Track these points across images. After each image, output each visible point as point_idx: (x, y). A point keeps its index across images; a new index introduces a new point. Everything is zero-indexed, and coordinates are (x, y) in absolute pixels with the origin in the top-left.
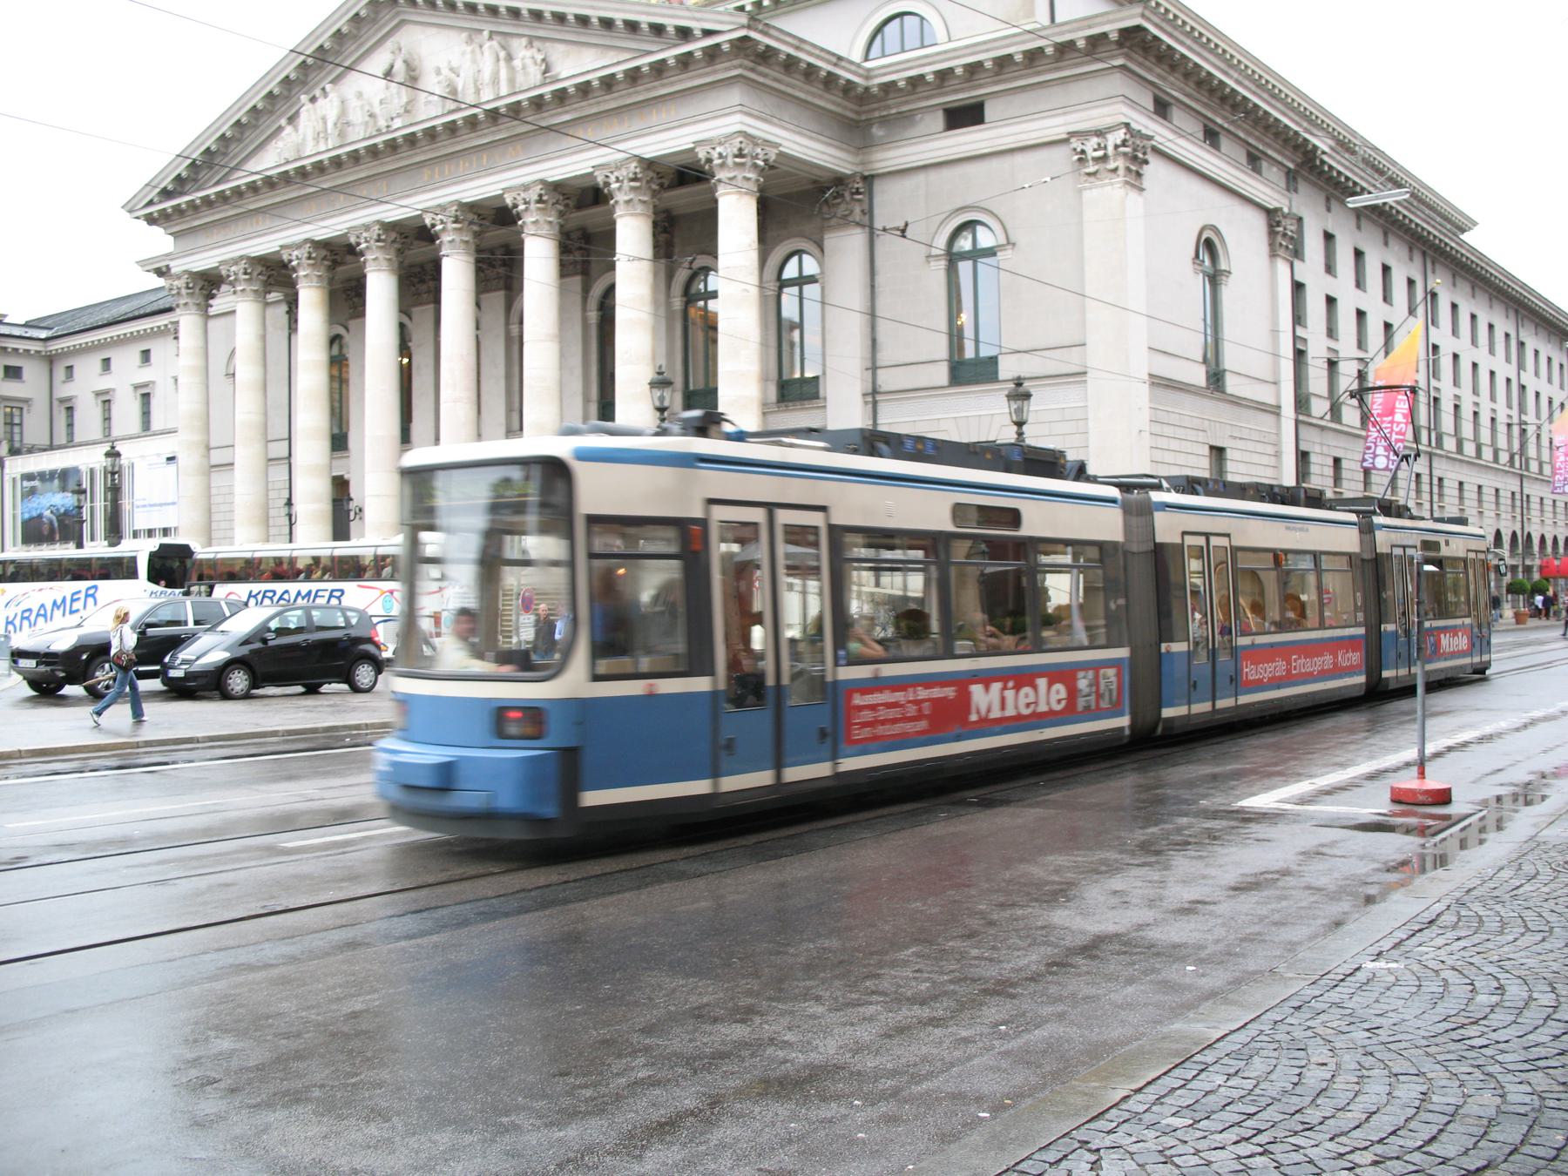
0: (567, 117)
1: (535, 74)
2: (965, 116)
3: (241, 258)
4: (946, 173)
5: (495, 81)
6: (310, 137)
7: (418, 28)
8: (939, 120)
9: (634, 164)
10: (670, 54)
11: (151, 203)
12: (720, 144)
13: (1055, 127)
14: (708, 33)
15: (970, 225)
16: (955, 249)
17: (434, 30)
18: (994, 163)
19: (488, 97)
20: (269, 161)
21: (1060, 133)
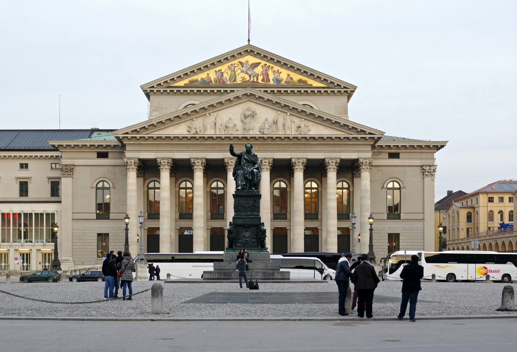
0: (316, 143)
2: (394, 156)
4: (387, 168)
6: (209, 127)
7: (254, 104)
8: (387, 156)
10: (359, 136)
11: (127, 133)
13: (419, 162)
15: (393, 181)
17: (261, 106)
18: (401, 168)
20: (180, 130)
21: (420, 164)
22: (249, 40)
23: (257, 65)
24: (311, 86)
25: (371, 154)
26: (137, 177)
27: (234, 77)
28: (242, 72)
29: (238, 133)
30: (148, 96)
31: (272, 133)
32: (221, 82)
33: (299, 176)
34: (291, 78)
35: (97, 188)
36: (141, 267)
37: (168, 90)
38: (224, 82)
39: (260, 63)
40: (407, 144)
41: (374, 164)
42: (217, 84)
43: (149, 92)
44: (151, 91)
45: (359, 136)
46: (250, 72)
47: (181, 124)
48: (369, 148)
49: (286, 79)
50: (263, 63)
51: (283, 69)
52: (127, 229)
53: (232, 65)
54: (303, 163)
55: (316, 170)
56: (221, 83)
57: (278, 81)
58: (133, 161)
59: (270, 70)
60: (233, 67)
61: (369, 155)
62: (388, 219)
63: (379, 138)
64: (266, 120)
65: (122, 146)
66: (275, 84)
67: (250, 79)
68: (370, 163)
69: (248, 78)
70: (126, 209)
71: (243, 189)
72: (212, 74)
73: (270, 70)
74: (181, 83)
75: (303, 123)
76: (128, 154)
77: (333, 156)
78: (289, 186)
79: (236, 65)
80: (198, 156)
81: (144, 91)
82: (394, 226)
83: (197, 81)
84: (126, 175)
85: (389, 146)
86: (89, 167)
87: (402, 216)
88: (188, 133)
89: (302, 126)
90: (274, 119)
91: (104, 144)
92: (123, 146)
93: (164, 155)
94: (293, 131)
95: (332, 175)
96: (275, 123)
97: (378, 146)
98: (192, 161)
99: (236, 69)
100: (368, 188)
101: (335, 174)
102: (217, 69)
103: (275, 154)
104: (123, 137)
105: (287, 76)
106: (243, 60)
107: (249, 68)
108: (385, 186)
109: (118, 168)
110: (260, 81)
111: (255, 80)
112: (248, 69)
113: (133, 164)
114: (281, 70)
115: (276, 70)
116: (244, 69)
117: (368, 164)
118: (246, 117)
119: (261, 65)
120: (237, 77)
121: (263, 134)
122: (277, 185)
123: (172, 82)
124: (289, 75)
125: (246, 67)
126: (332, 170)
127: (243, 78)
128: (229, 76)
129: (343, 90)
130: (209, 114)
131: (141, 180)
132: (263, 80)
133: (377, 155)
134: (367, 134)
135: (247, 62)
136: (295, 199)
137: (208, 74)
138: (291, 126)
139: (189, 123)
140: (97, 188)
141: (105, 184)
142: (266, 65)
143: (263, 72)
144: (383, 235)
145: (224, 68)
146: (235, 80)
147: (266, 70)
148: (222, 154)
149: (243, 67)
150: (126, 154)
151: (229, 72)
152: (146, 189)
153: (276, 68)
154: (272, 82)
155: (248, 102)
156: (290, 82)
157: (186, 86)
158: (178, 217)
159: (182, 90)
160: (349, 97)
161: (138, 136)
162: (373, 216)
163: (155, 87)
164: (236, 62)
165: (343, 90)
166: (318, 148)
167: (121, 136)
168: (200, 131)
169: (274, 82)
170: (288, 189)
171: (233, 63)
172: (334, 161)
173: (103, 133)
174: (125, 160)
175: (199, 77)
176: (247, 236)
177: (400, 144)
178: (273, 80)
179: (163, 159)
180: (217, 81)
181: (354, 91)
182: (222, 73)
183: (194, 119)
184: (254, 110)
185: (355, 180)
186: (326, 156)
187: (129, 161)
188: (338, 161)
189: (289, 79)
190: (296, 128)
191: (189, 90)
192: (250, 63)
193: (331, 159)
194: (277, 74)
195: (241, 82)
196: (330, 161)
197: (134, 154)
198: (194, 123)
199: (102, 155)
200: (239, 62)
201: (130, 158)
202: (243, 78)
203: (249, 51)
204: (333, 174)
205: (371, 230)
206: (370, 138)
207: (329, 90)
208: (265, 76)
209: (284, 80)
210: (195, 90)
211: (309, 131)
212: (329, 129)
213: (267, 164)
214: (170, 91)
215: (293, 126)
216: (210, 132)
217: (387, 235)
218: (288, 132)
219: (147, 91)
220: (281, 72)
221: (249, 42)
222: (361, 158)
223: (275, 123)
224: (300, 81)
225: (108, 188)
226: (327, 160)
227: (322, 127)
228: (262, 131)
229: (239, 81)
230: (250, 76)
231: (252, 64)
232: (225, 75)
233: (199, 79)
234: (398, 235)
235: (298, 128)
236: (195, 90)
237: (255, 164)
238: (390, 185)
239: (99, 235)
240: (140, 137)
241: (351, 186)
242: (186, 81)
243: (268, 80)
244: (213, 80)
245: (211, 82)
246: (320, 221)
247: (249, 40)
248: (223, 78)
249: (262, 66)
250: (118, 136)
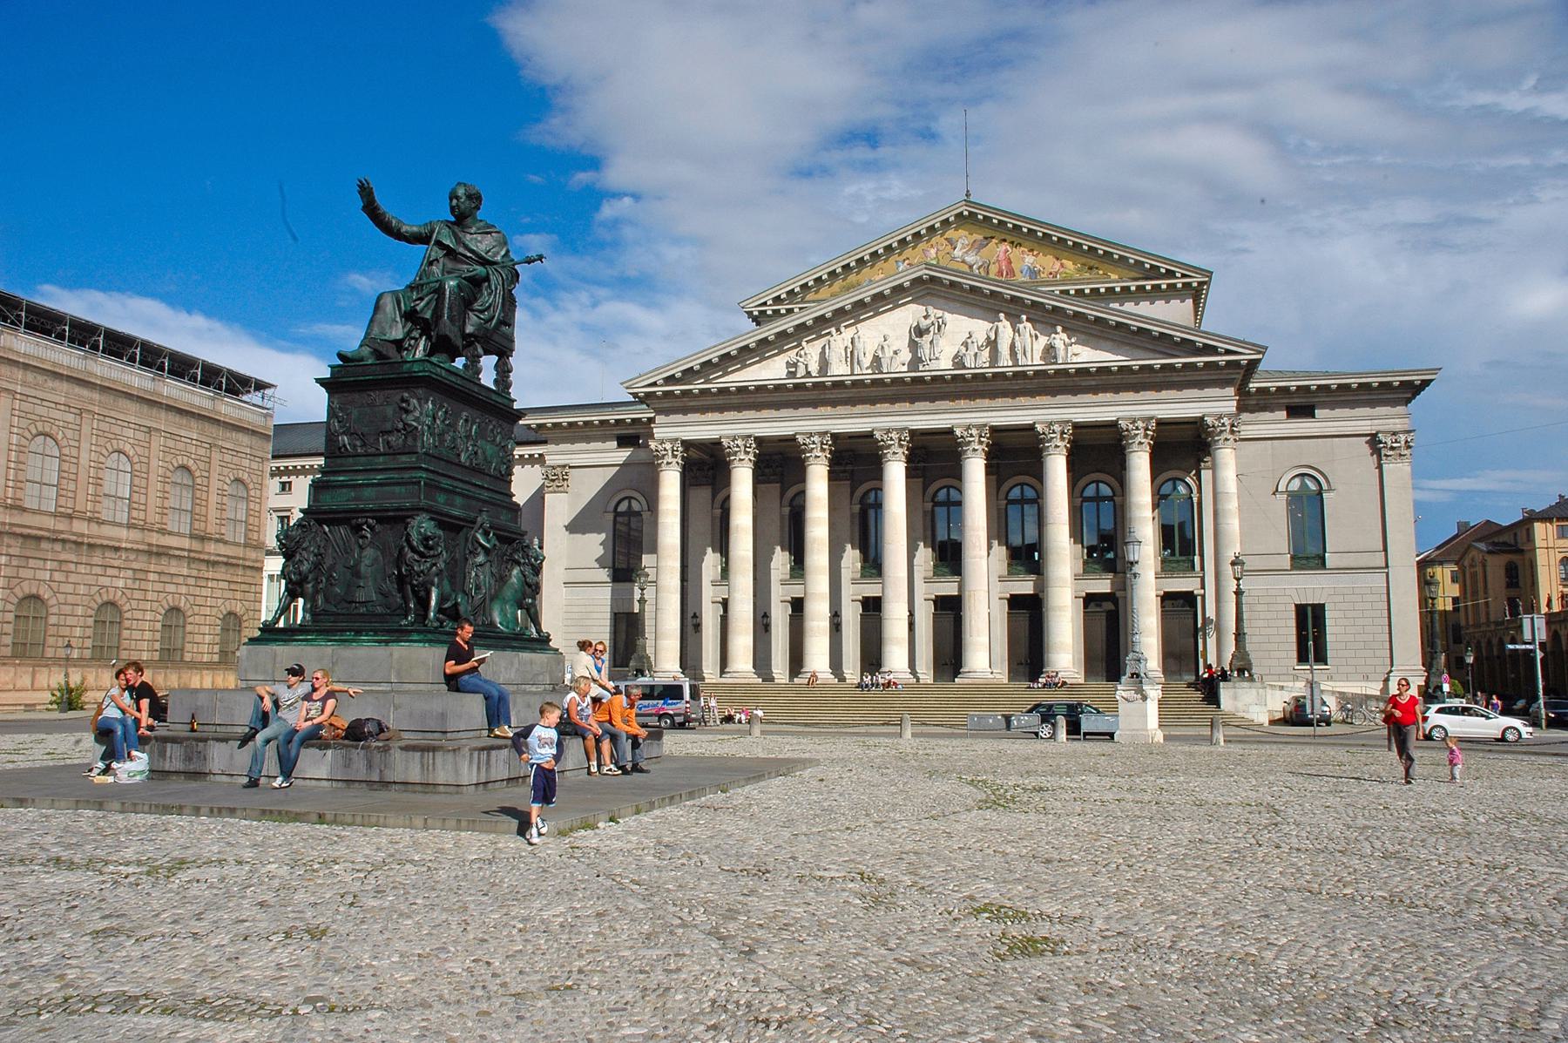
11: (654, 384)
13: (1367, 427)
14: (1228, 352)
15: (1302, 475)
20: (772, 371)
35: (617, 514)
45: (1200, 360)
46: (970, 259)
48: (1230, 391)
58: (668, 446)
61: (1231, 406)
62: (1293, 567)
76: (659, 432)
82: (1310, 587)
85: (1284, 391)
87: (1330, 559)
89: (1059, 344)
93: (736, 430)
97: (1258, 389)
110: (992, 276)
118: (920, 332)
121: (965, 368)
129: (1179, 283)
130: (838, 330)
132: (1000, 273)
141: (634, 503)
144: (1282, 607)
154: (1020, 278)
161: (677, 388)
165: (1179, 283)
205: (1239, 593)
206: (1228, 362)
207: (1148, 285)
223: (992, 344)
225: (638, 514)
234: (1319, 610)
243: (1011, 272)
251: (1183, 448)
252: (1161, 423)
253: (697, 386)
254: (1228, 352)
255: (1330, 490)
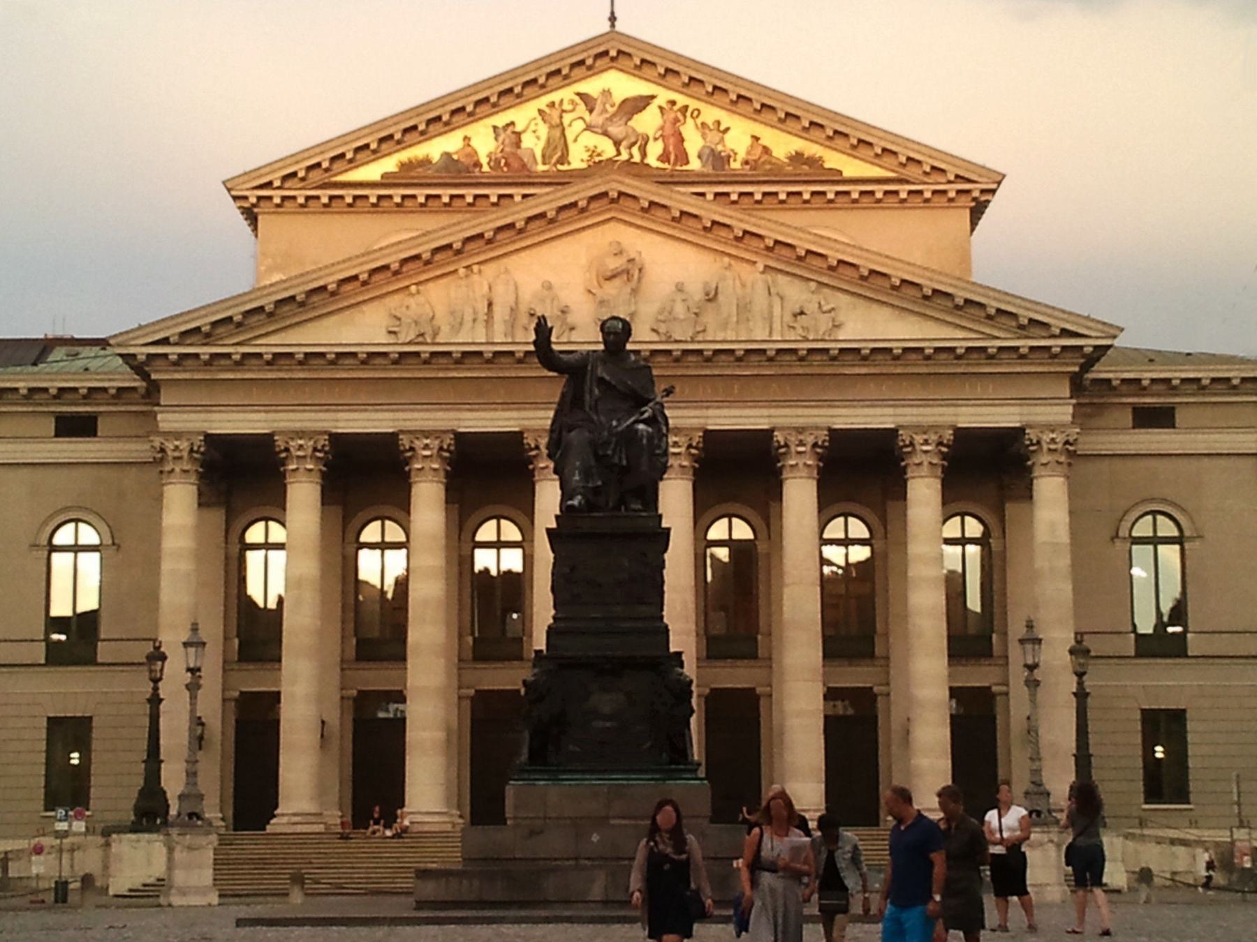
0: (864, 371)
1: (824, 323)
3: (325, 432)
4: (1130, 463)
5: (770, 319)
6: (468, 318)
7: (632, 230)
8: (1128, 419)
9: (951, 432)
10: (1024, 344)
11: (165, 341)
12: (1053, 431)
14: (1065, 333)
15: (1154, 513)
16: (1134, 534)
17: (658, 239)
19: (758, 333)
20: (363, 328)
22: (613, 19)
23: (639, 104)
24: (835, 177)
25: (1070, 409)
26: (200, 505)
27: (558, 147)
28: (589, 128)
29: (575, 337)
30: (251, 216)
31: (700, 338)
32: (515, 165)
33: (800, 494)
34: (766, 150)
36: (190, 848)
37: (324, 195)
38: (524, 166)
39: (653, 97)
40: (1205, 375)
41: (1082, 449)
42: (500, 173)
43: (256, 201)
44: (260, 198)
46: (615, 130)
47: (365, 308)
49: (748, 153)
50: (664, 96)
51: (736, 117)
52: (155, 701)
53: (552, 105)
54: (815, 445)
55: (862, 472)
56: (513, 171)
57: (718, 159)
58: (184, 445)
59: (689, 121)
60: (555, 114)
61: (1064, 413)
63: (1101, 350)
64: (680, 288)
65: (147, 389)
66: (709, 170)
67: (619, 154)
68: (1067, 443)
69: (608, 149)
70: (156, 626)
71: (590, 506)
72: (482, 140)
73: (689, 121)
74: (371, 172)
75: (815, 298)
76: (168, 421)
77: (924, 418)
78: (763, 534)
79: (566, 106)
80: (424, 422)
81: (235, 198)
83: (426, 162)
84: (159, 498)
86: (24, 472)
88: (392, 339)
89: (811, 308)
90: (706, 284)
91: (84, 384)
92: (153, 390)
93: (299, 422)
94: (777, 325)
95: (924, 492)
96: (711, 297)
97: (1095, 381)
98: (405, 441)
99: (567, 118)
100: (1064, 536)
101: (937, 484)
102: (500, 120)
103: (711, 412)
104: (150, 357)
105: (748, 141)
106: (592, 86)
107: (614, 115)
108: (1123, 532)
109: (134, 470)
110: (652, 160)
111: (637, 158)
112: (610, 119)
113: (185, 454)
114: (727, 119)
115: (710, 122)
116: (596, 119)
117: (1060, 446)
119: (656, 102)
120: (572, 147)
122: (718, 531)
123: (338, 166)
124: (756, 138)
125: (604, 110)
126: (925, 469)
127: (593, 152)
128: (542, 144)
131: (217, 517)
132: (664, 157)
133: (1090, 416)
134: (1053, 336)
135: (607, 93)
136: (788, 579)
137: (466, 139)
138: (768, 310)
139: (393, 302)
140: (54, 549)
142: (673, 103)
143: (662, 128)
145: (523, 115)
146: (563, 159)
147: (676, 120)
148: (514, 414)
149: (591, 111)
150: (159, 417)
151: (543, 130)
152: (235, 549)
153: (711, 114)
154: (695, 164)
155: (612, 224)
156: (762, 168)
157: (388, 181)
158: (351, 653)
159: (373, 195)
160: (977, 211)
162: (1088, 642)
163: (277, 183)
164: (565, 95)
166: (871, 390)
167: (142, 352)
168: (435, 334)
169: (703, 166)
170: (762, 547)
171: (555, 97)
172: (933, 438)
173: (87, 351)
174: (157, 441)
175: (436, 148)
176: (607, 709)
177: (1176, 375)
178: (700, 157)
179: (301, 434)
180: (498, 161)
181: (993, 191)
182: (518, 134)
183: (413, 288)
184: (632, 256)
185: (1011, 509)
186: (902, 420)
187: (170, 446)
188: (948, 435)
189: (759, 151)
190: (788, 318)
191: (397, 194)
192: (618, 97)
193: (924, 429)
194: (713, 137)
195: (584, 165)
196: (919, 439)
197: (190, 419)
198: (412, 302)
199: (76, 426)
200: (578, 94)
201: (178, 435)
202: (593, 152)
203: (613, 53)
204: (928, 487)
207: (903, 190)
208: (672, 140)
209: (742, 155)
210: (421, 194)
211: (837, 326)
212: (913, 319)
213: (682, 450)
214: (331, 198)
215: (777, 311)
216: (473, 336)
217: (1138, 716)
218: (760, 333)
219: (246, 198)
220: (727, 129)
221: (613, 26)
222: (1031, 427)
224: (797, 158)
226: (904, 435)
227: (886, 312)
228: (662, 328)
229: (577, 160)
230: (617, 144)
231: (624, 102)
232: (528, 141)
233: (436, 157)
235: (795, 315)
236: (421, 194)
237: (646, 402)
238: (1143, 528)
239: (54, 723)
240: (214, 356)
241: (996, 533)
242: (389, 164)
244: (484, 161)
245: (478, 164)
246: (882, 662)
247: (613, 19)
248: (519, 151)
249: (661, 108)
250: (132, 350)
251: (988, 470)
252: (959, 433)
253: (230, 347)
254: (1065, 333)
255: (1192, 538)
